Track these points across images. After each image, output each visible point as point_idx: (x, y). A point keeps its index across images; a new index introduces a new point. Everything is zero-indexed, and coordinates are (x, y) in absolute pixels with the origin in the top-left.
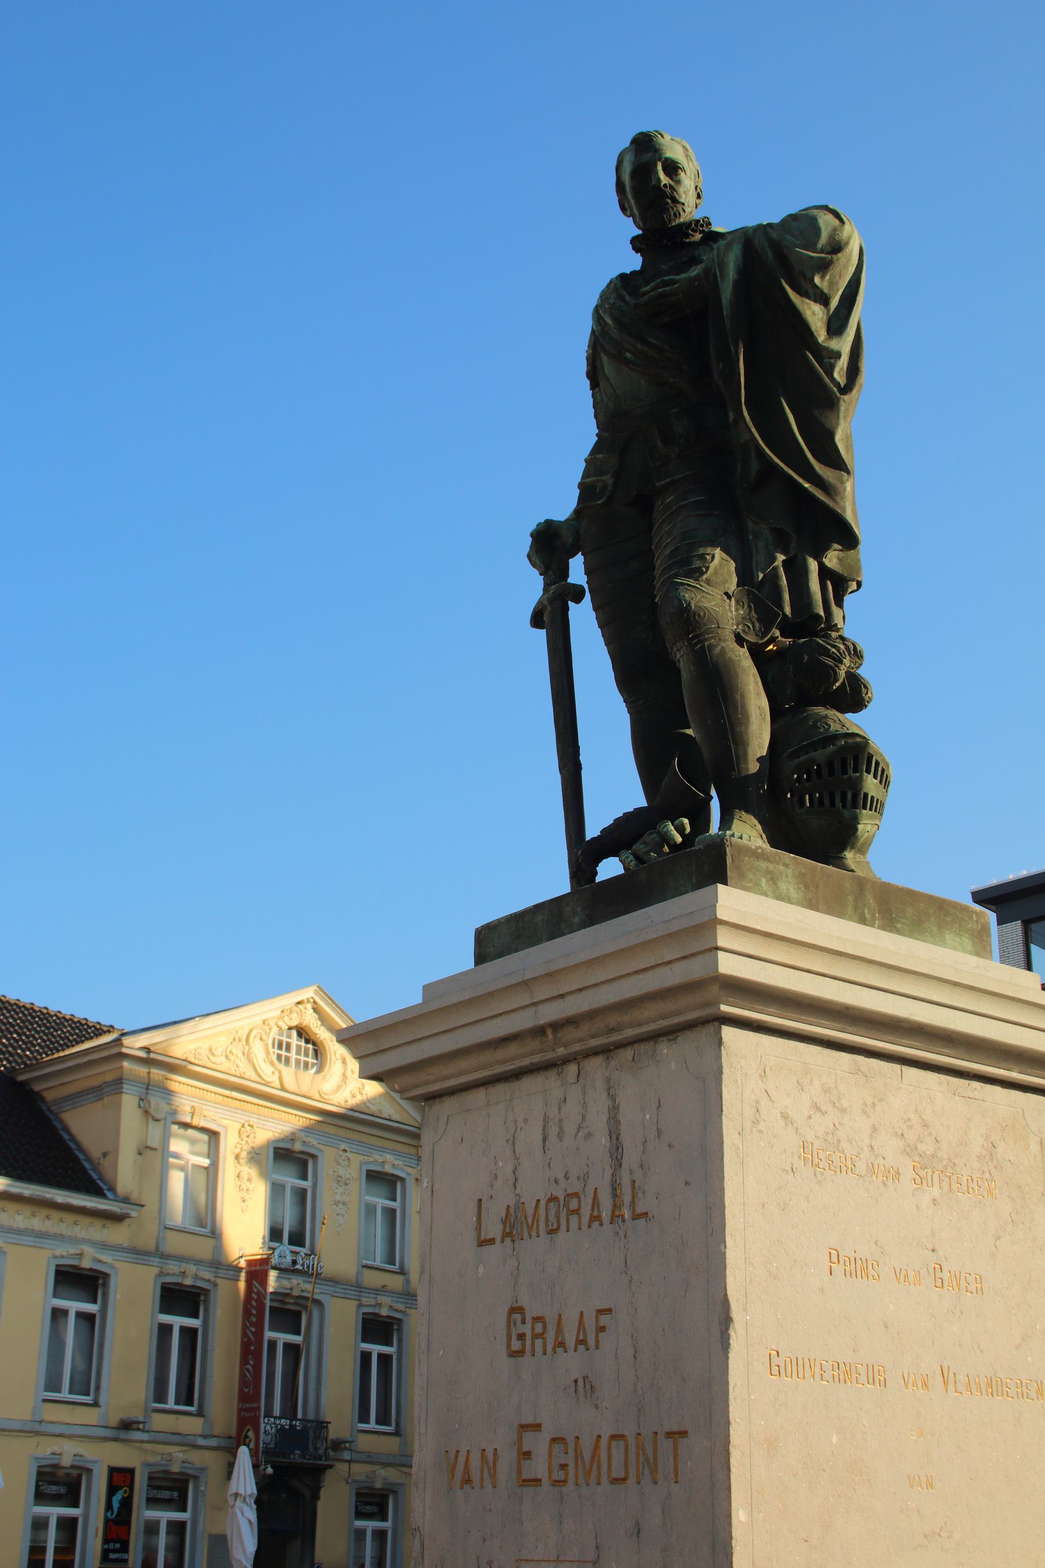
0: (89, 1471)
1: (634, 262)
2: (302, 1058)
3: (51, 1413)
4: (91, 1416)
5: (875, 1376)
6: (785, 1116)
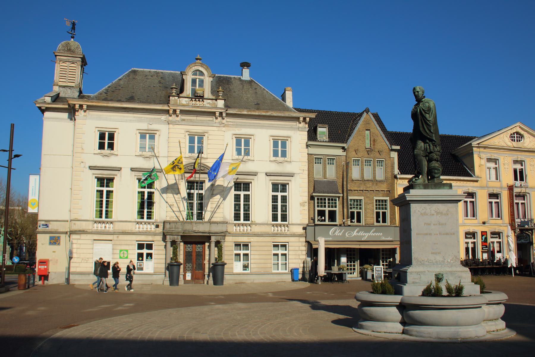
0: (477, 233)
1: (417, 102)
2: (518, 139)
3: (466, 221)
4: (476, 221)
5: (430, 234)
6: (418, 211)
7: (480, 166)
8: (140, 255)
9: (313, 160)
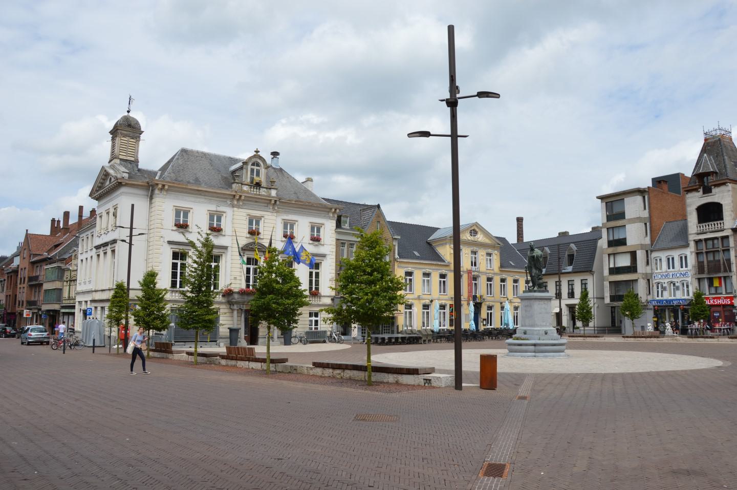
3: (441, 296)
9: (340, 243)
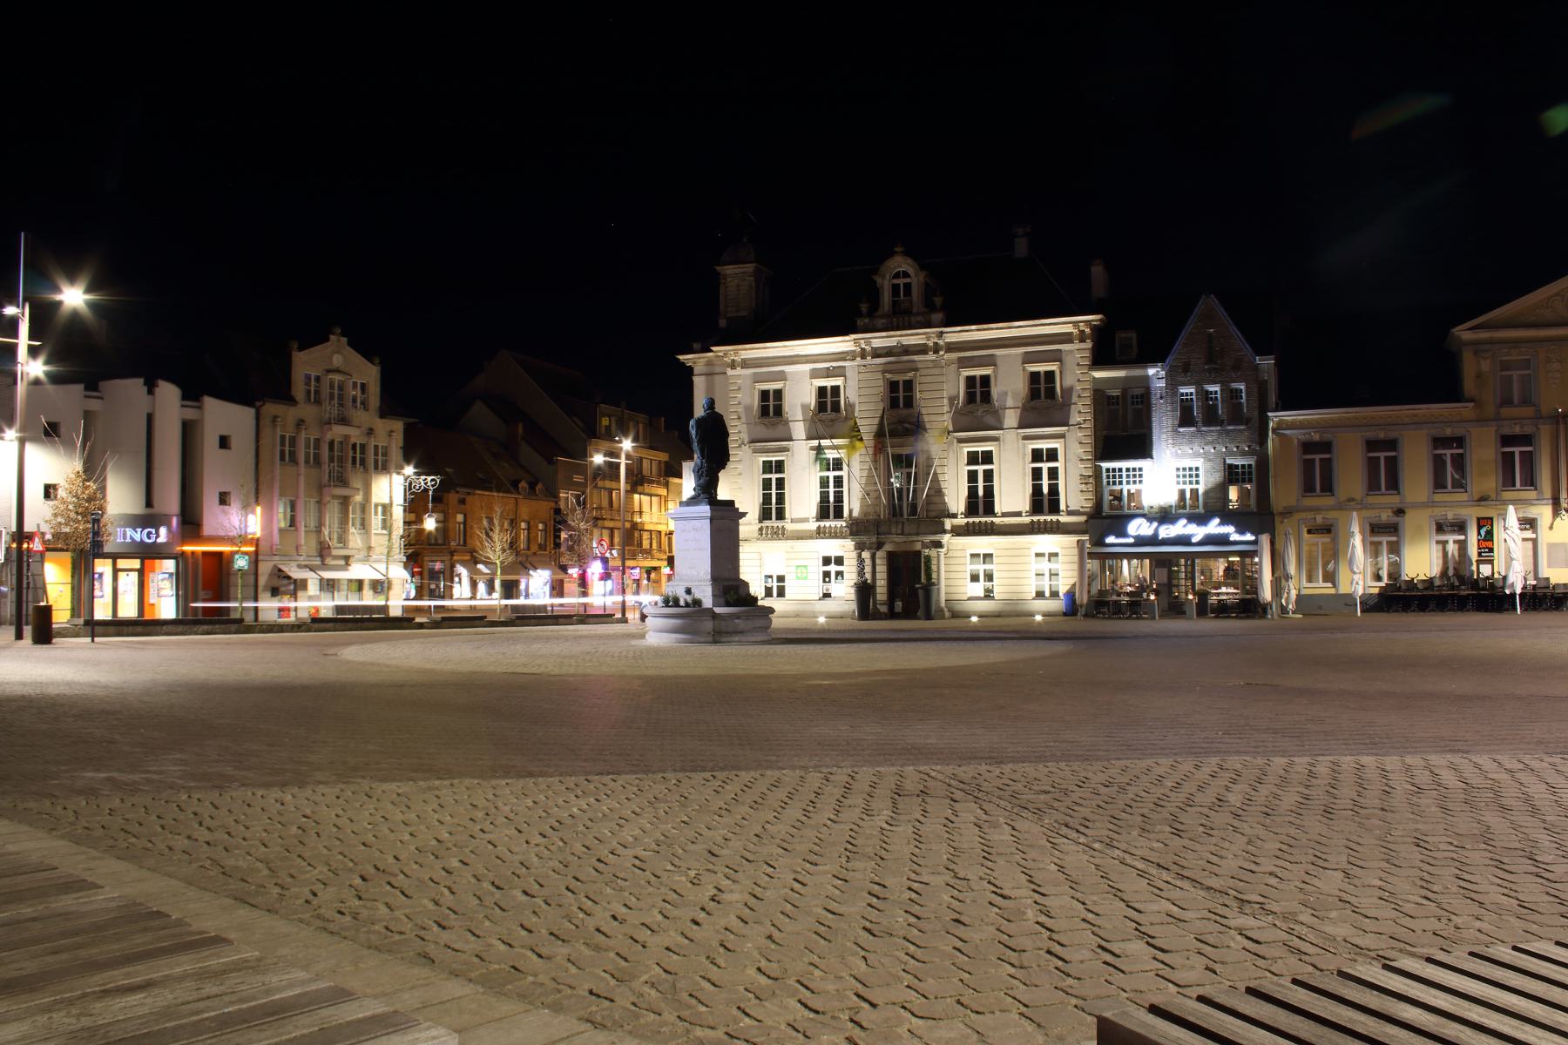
7: (1479, 376)
8: (827, 575)
